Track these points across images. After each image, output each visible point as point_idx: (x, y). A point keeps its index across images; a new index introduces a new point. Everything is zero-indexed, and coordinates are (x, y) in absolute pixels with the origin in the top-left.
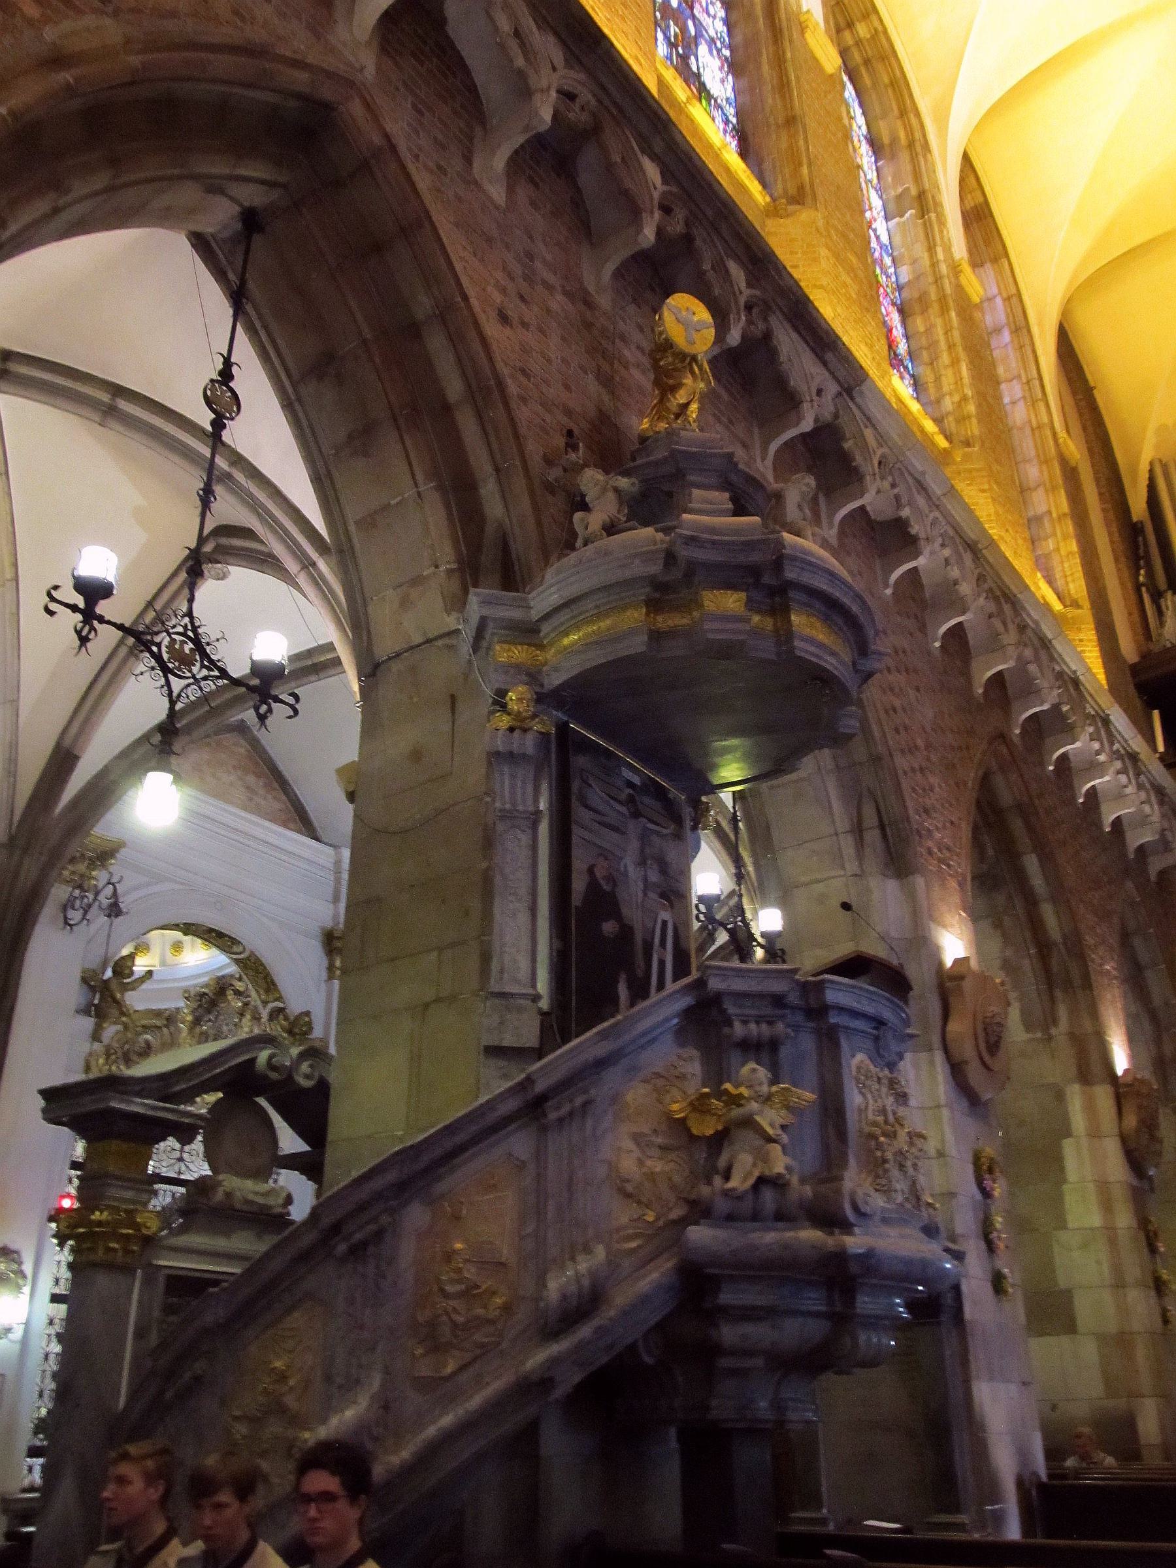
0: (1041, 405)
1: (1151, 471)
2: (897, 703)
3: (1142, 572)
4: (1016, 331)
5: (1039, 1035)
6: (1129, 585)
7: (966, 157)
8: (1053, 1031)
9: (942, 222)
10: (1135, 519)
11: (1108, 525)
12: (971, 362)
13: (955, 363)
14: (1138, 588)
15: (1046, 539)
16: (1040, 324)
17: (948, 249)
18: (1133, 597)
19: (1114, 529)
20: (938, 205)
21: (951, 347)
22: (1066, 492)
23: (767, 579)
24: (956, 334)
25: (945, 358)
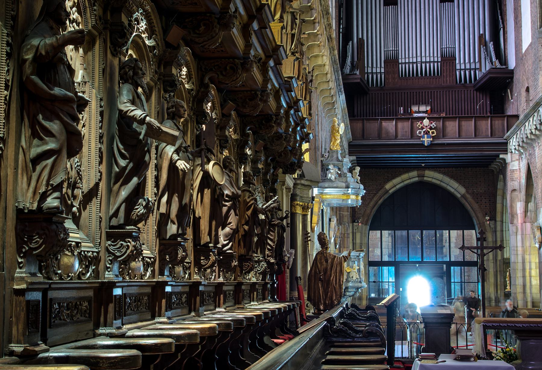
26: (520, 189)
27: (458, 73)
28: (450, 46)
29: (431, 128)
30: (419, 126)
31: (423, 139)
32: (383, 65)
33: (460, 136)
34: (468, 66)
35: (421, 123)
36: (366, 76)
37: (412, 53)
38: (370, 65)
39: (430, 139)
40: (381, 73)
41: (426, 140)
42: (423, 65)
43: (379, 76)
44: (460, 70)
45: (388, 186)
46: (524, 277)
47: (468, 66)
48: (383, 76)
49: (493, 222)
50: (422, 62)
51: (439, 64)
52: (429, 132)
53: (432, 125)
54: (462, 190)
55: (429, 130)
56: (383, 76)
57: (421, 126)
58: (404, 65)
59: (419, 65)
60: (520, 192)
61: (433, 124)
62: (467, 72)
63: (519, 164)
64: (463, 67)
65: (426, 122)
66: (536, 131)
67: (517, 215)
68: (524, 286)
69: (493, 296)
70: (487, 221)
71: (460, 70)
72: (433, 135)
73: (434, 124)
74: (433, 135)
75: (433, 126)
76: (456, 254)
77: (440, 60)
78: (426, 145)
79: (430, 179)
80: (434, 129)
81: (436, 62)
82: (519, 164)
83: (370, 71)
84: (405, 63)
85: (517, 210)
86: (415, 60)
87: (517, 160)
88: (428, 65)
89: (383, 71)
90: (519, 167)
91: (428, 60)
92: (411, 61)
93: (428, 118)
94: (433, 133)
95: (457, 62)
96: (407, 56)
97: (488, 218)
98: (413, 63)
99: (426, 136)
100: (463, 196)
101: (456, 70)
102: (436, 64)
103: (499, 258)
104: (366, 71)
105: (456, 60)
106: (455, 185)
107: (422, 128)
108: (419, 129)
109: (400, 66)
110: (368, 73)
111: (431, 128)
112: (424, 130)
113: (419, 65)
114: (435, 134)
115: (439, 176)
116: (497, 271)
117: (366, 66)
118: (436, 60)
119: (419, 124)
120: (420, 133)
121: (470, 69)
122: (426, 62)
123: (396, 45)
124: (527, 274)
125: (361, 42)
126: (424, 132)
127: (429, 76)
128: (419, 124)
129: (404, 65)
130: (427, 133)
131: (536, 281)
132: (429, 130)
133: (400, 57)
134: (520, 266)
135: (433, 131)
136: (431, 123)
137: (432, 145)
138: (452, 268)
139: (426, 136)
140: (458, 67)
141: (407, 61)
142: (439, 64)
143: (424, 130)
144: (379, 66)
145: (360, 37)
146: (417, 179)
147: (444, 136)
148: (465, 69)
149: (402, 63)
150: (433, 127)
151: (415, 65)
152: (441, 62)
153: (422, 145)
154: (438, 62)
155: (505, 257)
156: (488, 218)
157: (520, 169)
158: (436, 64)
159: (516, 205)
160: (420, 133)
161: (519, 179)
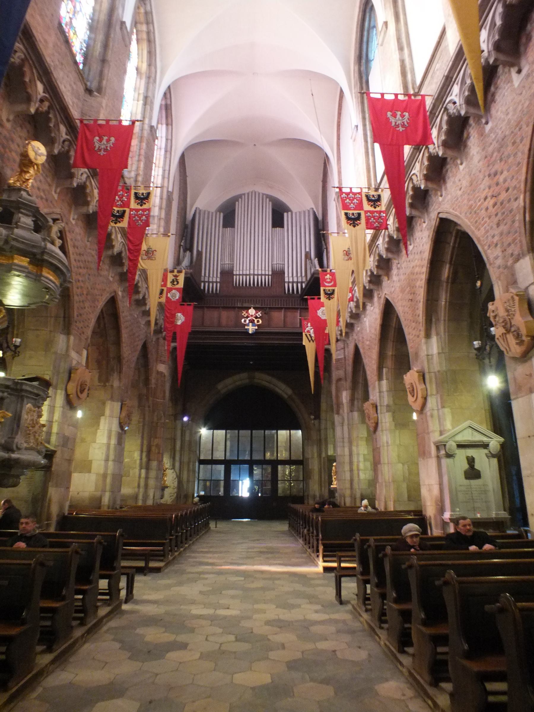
0: (166, 180)
1: (196, 211)
3: (183, 241)
4: (166, 151)
6: (177, 245)
7: (169, 87)
9: (152, 110)
10: (187, 223)
11: (177, 222)
13: (139, 161)
14: (180, 246)
15: (154, 224)
16: (175, 153)
17: (151, 119)
18: (177, 249)
19: (178, 225)
20: (152, 103)
22: (165, 211)
23: (38, 257)
24: (143, 152)
26: (346, 377)
27: (286, 285)
29: (256, 317)
34: (295, 280)
35: (247, 312)
37: (246, 265)
38: (207, 275)
39: (254, 328)
41: (251, 329)
42: (256, 277)
44: (289, 282)
45: (220, 386)
46: (351, 470)
47: (295, 280)
48: (218, 285)
49: (316, 422)
50: (254, 275)
51: (270, 277)
52: (254, 320)
53: (257, 315)
54: (289, 392)
55: (254, 319)
57: (246, 315)
58: (238, 277)
59: (252, 277)
60: (346, 380)
61: (259, 313)
62: (295, 285)
63: (344, 353)
64: (291, 280)
65: (252, 311)
66: (371, 285)
67: (343, 405)
68: (352, 481)
69: (317, 494)
70: (311, 420)
71: (289, 282)
73: (259, 314)
76: (283, 455)
77: (270, 273)
78: (250, 332)
79: (259, 381)
80: (259, 318)
82: (344, 353)
84: (239, 275)
85: (342, 400)
86: (248, 273)
88: (260, 277)
89: (218, 280)
90: (345, 355)
91: (260, 273)
92: (244, 273)
93: (254, 308)
94: (258, 321)
95: (286, 275)
96: (241, 269)
97: (312, 417)
98: (246, 275)
99: (251, 324)
100: (290, 397)
101: (285, 282)
103: (323, 455)
104: (202, 280)
105: (284, 273)
106: (283, 386)
107: (247, 317)
108: (245, 318)
109: (235, 277)
110: (204, 282)
111: (256, 317)
115: (269, 378)
116: (321, 468)
117: (203, 275)
118: (267, 273)
119: (244, 313)
120: (245, 321)
121: (297, 282)
122: (258, 275)
123: (232, 259)
124: (355, 467)
125: (199, 254)
126: (249, 320)
127: (261, 287)
128: (244, 313)
129: (238, 277)
130: (252, 321)
131: (364, 475)
132: (254, 319)
133: (235, 269)
134: (347, 459)
136: (257, 313)
137: (256, 333)
138: (279, 467)
140: (286, 280)
144: (215, 276)
146: (247, 381)
147: (269, 326)
148: (293, 282)
149: (236, 275)
151: (248, 277)
152: (271, 275)
153: (246, 333)
154: (268, 275)
155: (329, 454)
156: (312, 417)
157: (345, 357)
159: (342, 394)
160: (245, 321)
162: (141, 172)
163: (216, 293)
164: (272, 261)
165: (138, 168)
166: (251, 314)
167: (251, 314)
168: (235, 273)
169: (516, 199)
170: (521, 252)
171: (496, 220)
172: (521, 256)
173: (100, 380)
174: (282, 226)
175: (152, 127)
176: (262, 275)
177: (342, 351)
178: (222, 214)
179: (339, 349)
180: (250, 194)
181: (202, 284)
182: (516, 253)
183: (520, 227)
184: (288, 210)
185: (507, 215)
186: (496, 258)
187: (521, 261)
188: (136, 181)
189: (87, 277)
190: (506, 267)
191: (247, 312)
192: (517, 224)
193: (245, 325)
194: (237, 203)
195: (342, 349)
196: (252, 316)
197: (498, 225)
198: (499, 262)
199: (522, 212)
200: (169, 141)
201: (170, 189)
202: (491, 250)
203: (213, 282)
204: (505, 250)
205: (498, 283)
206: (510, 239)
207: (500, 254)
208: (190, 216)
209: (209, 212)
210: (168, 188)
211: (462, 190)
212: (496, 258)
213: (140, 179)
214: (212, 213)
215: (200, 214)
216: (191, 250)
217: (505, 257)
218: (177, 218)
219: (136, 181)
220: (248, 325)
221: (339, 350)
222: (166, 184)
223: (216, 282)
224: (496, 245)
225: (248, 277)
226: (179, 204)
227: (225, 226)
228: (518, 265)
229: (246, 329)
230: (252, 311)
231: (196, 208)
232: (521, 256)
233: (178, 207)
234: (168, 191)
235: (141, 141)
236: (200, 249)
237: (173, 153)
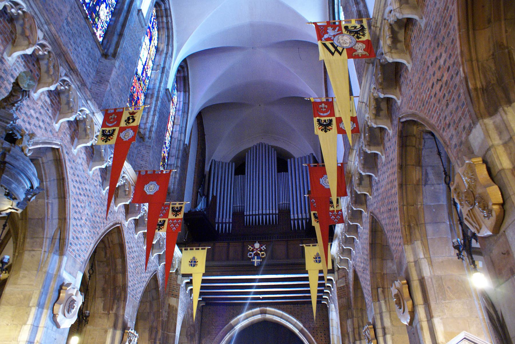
0: (183, 135)
2: (79, 205)
4: (184, 112)
5: (106, 312)
8: (111, 312)
9: (167, 77)
12: (159, 117)
13: (154, 115)
14: (197, 192)
20: (168, 72)
21: (155, 110)
22: (181, 161)
25: (152, 113)
28: (286, 202)
30: (250, 249)
31: (253, 260)
32: (231, 216)
33: (288, 257)
36: (217, 225)
38: (221, 217)
39: (259, 260)
40: (229, 223)
42: (264, 216)
43: (228, 225)
44: (294, 219)
48: (231, 225)
50: (263, 214)
51: (277, 215)
53: (262, 248)
56: (231, 225)
57: (252, 248)
61: (264, 247)
65: (257, 245)
71: (294, 219)
72: (263, 257)
74: (263, 257)
75: (263, 248)
77: (277, 212)
78: (255, 265)
81: (274, 214)
83: (220, 221)
86: (257, 213)
87: (343, 277)
89: (231, 221)
95: (292, 213)
98: (256, 215)
101: (291, 219)
102: (274, 216)
104: (217, 221)
105: (290, 212)
107: (253, 251)
109: (245, 217)
110: (218, 223)
111: (261, 251)
112: (254, 252)
113: (261, 217)
114: (265, 256)
117: (217, 217)
122: (266, 214)
123: (243, 201)
125: (214, 198)
130: (257, 254)
133: (246, 210)
135: (262, 253)
136: (262, 247)
139: (256, 257)
141: (251, 213)
142: (277, 215)
143: (254, 252)
145: (215, 195)
148: (298, 219)
149: (247, 215)
150: (263, 250)
151: (257, 217)
152: (278, 214)
154: (276, 214)
158: (274, 216)
161: (347, 295)
162: (155, 124)
163: (229, 233)
164: (279, 201)
165: (153, 121)
166: (256, 248)
167: (256, 248)
168: (245, 213)
169: (457, 74)
170: (471, 122)
171: (444, 102)
172: (472, 125)
173: (104, 308)
174: (287, 171)
175: (167, 90)
176: (269, 214)
177: (344, 279)
178: (234, 164)
179: (340, 277)
180: (258, 148)
181: (217, 225)
182: (467, 125)
183: (465, 99)
184: (290, 156)
185: (453, 92)
186: (451, 139)
187: (474, 130)
188: (150, 131)
189: (87, 203)
190: (461, 143)
191: (252, 247)
192: (463, 97)
193: (250, 259)
194: (247, 154)
195: (343, 277)
196: (257, 249)
197: (447, 105)
198: (454, 141)
199: (464, 83)
200: (187, 105)
201: (187, 142)
202: (446, 132)
203: (226, 223)
204: (457, 127)
205: (457, 162)
206: (460, 114)
207: (454, 133)
208: (207, 169)
209: (222, 163)
210: (184, 141)
211: (414, 88)
212: (451, 139)
213: (154, 129)
214: (226, 164)
215: (215, 164)
216: (207, 197)
217: (458, 133)
218: (195, 168)
219: (150, 131)
220: (253, 258)
221: (341, 278)
222: (183, 138)
223: (229, 223)
224: (449, 124)
225: (257, 217)
226: (197, 157)
227: (236, 173)
228: (471, 136)
229: (252, 262)
230: (257, 245)
231: (212, 160)
232: (472, 125)
233: (196, 160)
234: (184, 144)
235: (157, 100)
236: (215, 195)
237: (189, 115)
